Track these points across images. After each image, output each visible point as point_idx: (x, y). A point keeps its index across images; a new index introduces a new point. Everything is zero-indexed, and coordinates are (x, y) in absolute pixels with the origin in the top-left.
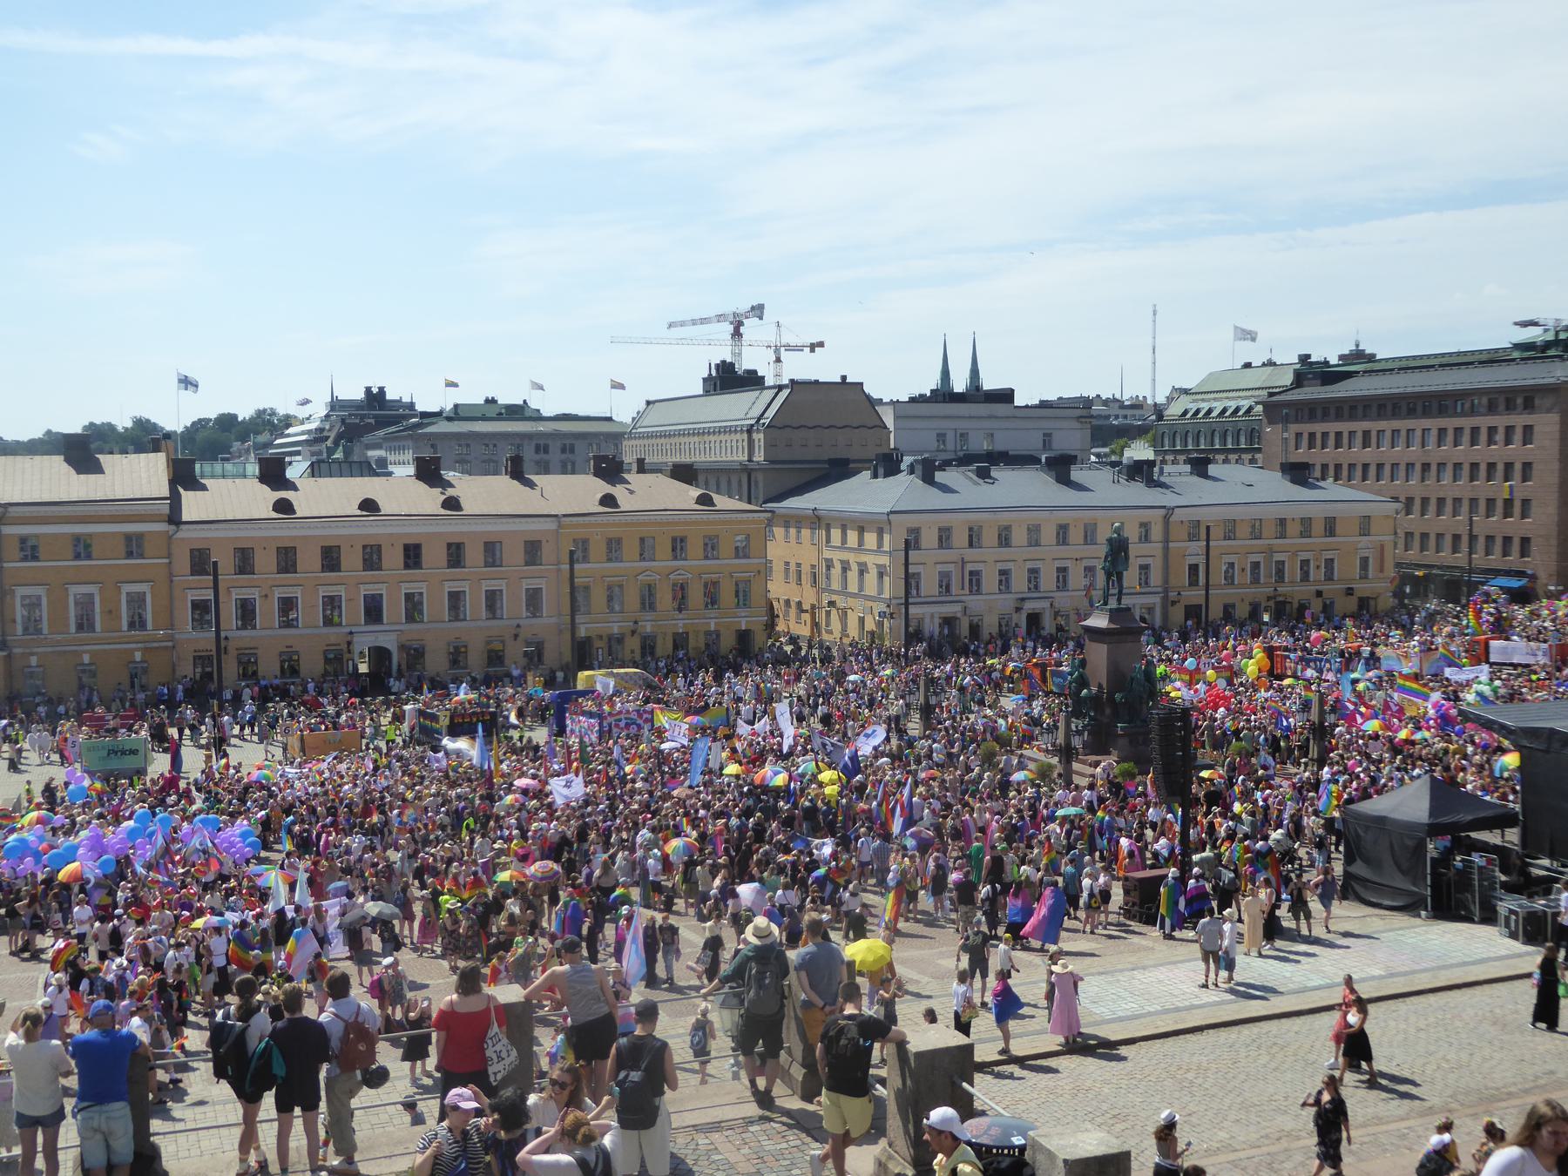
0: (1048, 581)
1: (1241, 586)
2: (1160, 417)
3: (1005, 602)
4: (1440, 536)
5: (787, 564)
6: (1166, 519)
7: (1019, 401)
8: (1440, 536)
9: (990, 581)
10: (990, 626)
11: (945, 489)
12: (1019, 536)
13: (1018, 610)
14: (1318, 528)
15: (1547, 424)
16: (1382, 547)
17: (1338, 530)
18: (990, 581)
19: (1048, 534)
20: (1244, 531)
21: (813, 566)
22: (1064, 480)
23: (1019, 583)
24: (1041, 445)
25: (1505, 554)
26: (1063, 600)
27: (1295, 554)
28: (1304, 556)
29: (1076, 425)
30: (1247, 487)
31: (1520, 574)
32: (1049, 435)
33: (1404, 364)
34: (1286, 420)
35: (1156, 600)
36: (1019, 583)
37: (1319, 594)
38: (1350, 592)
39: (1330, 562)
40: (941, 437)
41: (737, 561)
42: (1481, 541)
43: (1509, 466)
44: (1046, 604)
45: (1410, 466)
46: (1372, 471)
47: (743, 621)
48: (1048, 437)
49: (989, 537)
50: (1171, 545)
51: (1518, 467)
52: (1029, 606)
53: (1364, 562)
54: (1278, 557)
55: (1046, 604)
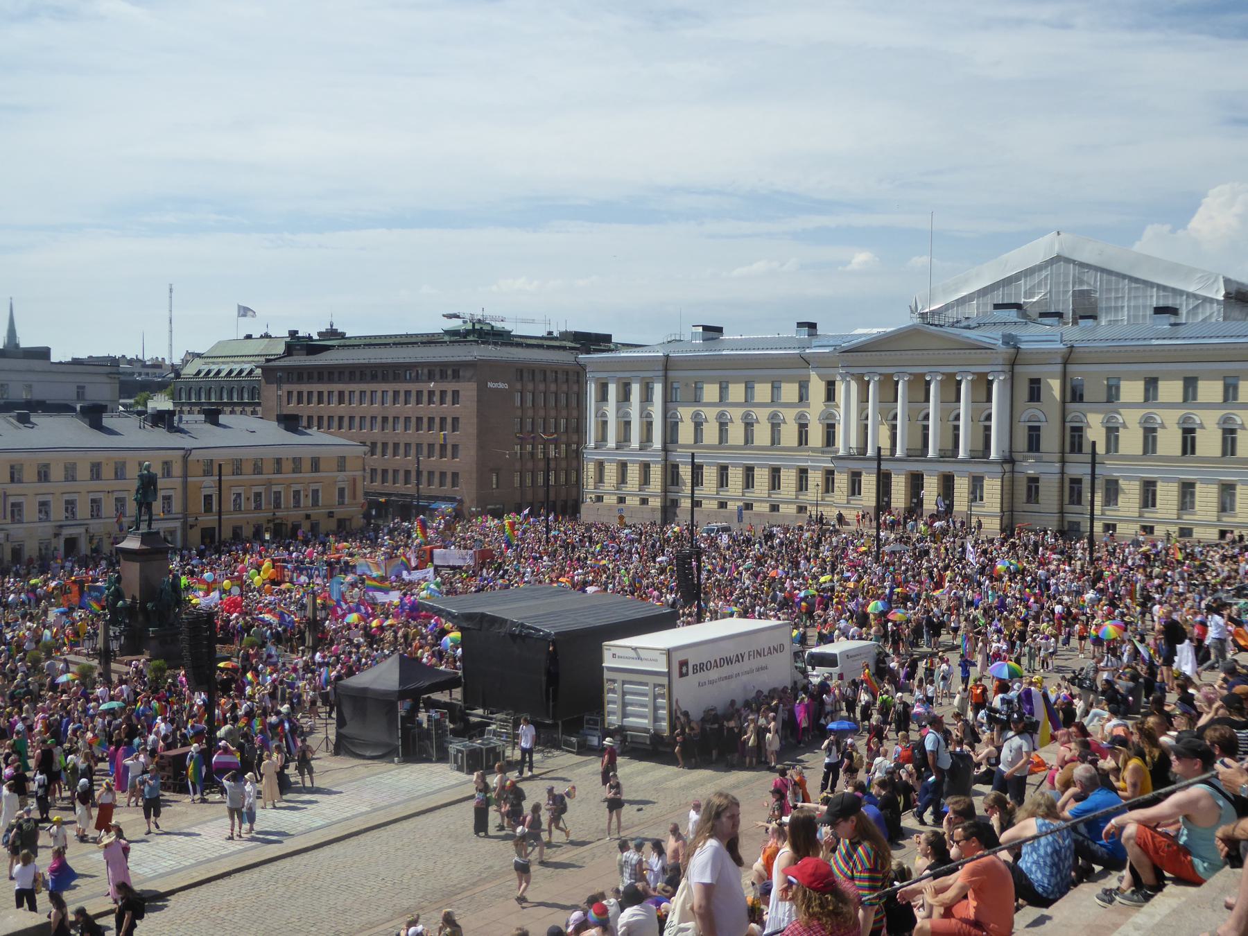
0: (83, 511)
1: (248, 512)
2: (178, 375)
3: (45, 529)
4: (395, 472)
6: (185, 459)
7: (55, 358)
8: (395, 472)
10: (31, 549)
12: (57, 473)
13: (56, 535)
14: (306, 465)
15: (468, 390)
16: (354, 480)
17: (322, 467)
18: (30, 511)
19: (83, 472)
20: (248, 468)
22: (97, 425)
24: (75, 397)
25: (442, 484)
26: (96, 526)
27: (289, 486)
28: (297, 487)
29: (108, 380)
30: (250, 433)
31: (452, 500)
32: (83, 387)
33: (368, 341)
34: (279, 382)
35: (178, 524)
37: (308, 517)
38: (331, 515)
39: (315, 492)
42: (425, 474)
43: (443, 420)
44: (82, 530)
46: (346, 422)
49: (30, 474)
51: (449, 421)
52: (67, 532)
53: (342, 491)
54: (275, 488)
55: (82, 530)
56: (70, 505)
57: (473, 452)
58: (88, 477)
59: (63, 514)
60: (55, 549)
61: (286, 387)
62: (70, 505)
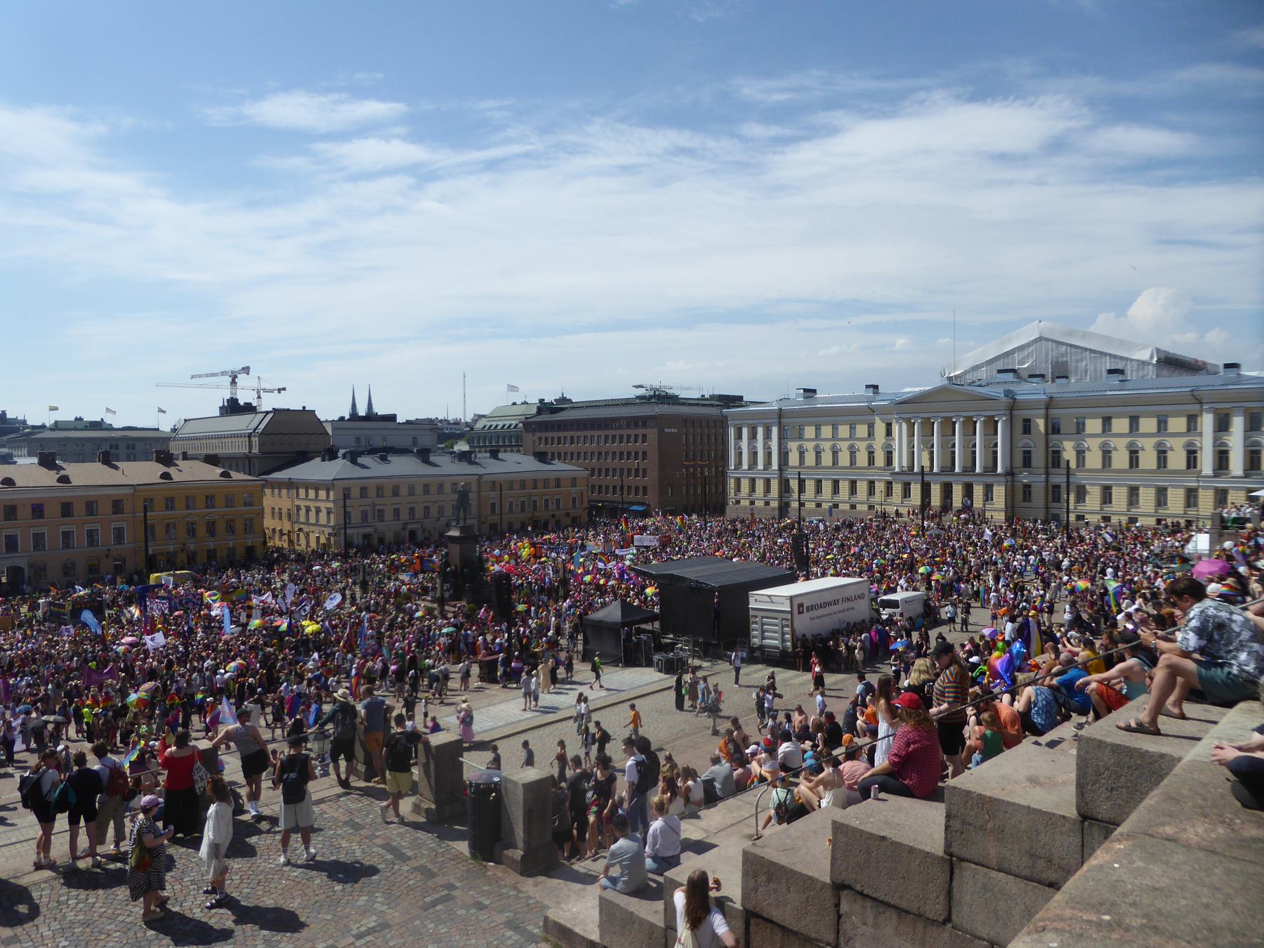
2: (472, 429)
4: (607, 487)
7: (400, 419)
8: (607, 487)
9: (389, 514)
10: (389, 537)
11: (363, 467)
13: (404, 529)
14: (553, 484)
18: (389, 514)
20: (540, 484)
22: (426, 461)
23: (404, 516)
30: (518, 464)
31: (643, 504)
34: (534, 431)
35: (475, 522)
36: (404, 516)
38: (568, 514)
39: (558, 500)
40: (358, 440)
43: (637, 453)
45: (592, 453)
49: (388, 492)
52: (410, 527)
53: (574, 499)
56: (412, 510)
57: (656, 474)
59: (407, 517)
61: (538, 435)
62: (412, 510)
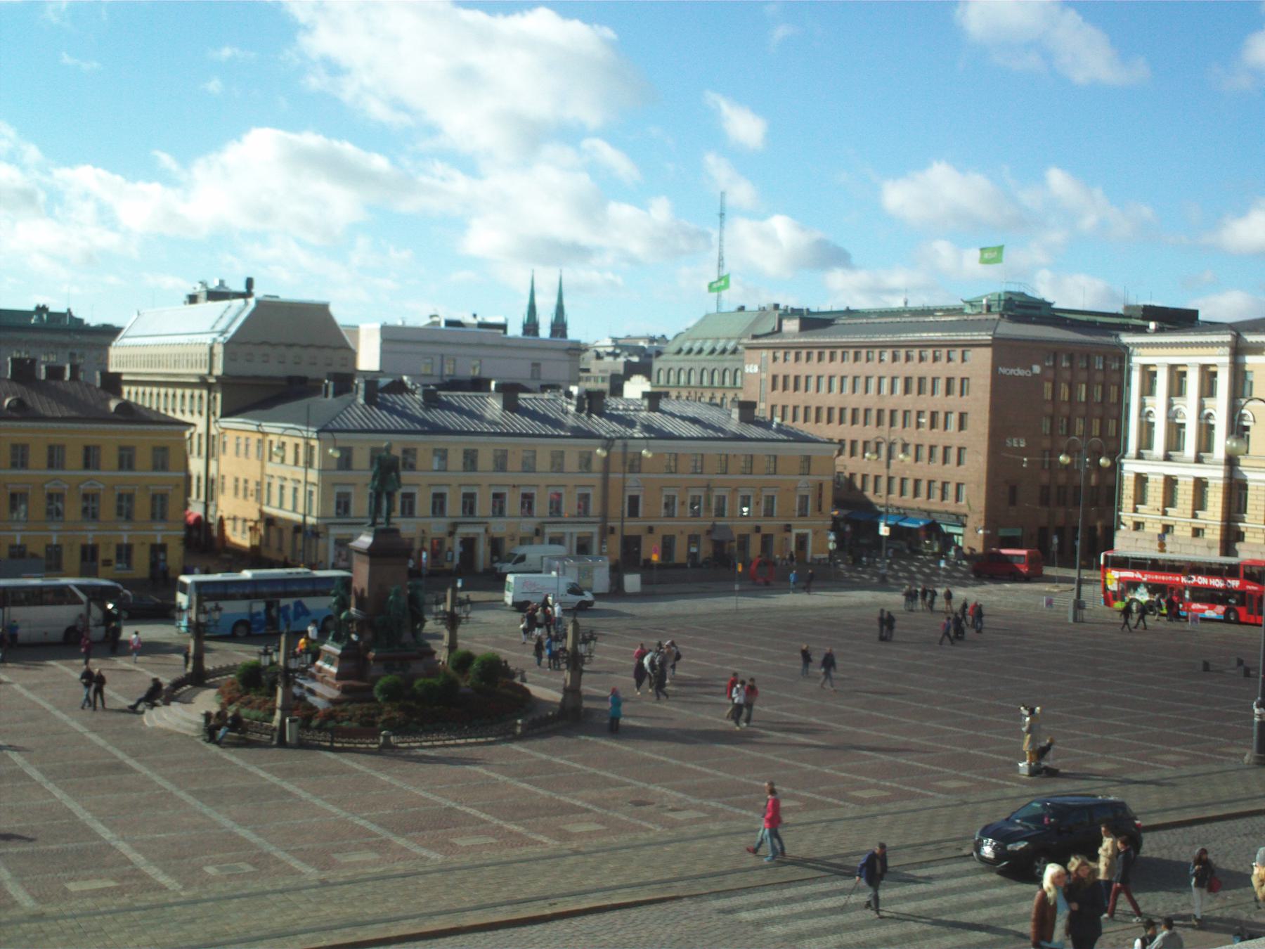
5: (237, 480)
13: (451, 534)
16: (821, 485)
21: (258, 484)
23: (454, 507)
27: (736, 490)
28: (671, 492)
35: (595, 529)
36: (454, 507)
37: (758, 529)
39: (770, 500)
41: (15, 472)
44: (481, 530)
45: (920, 414)
47: (90, 535)
48: (536, 365)
50: (611, 476)
52: (463, 531)
53: (804, 499)
54: (718, 492)
56: (469, 502)
58: (548, 468)
59: (458, 510)
60: (450, 550)
62: (469, 502)
